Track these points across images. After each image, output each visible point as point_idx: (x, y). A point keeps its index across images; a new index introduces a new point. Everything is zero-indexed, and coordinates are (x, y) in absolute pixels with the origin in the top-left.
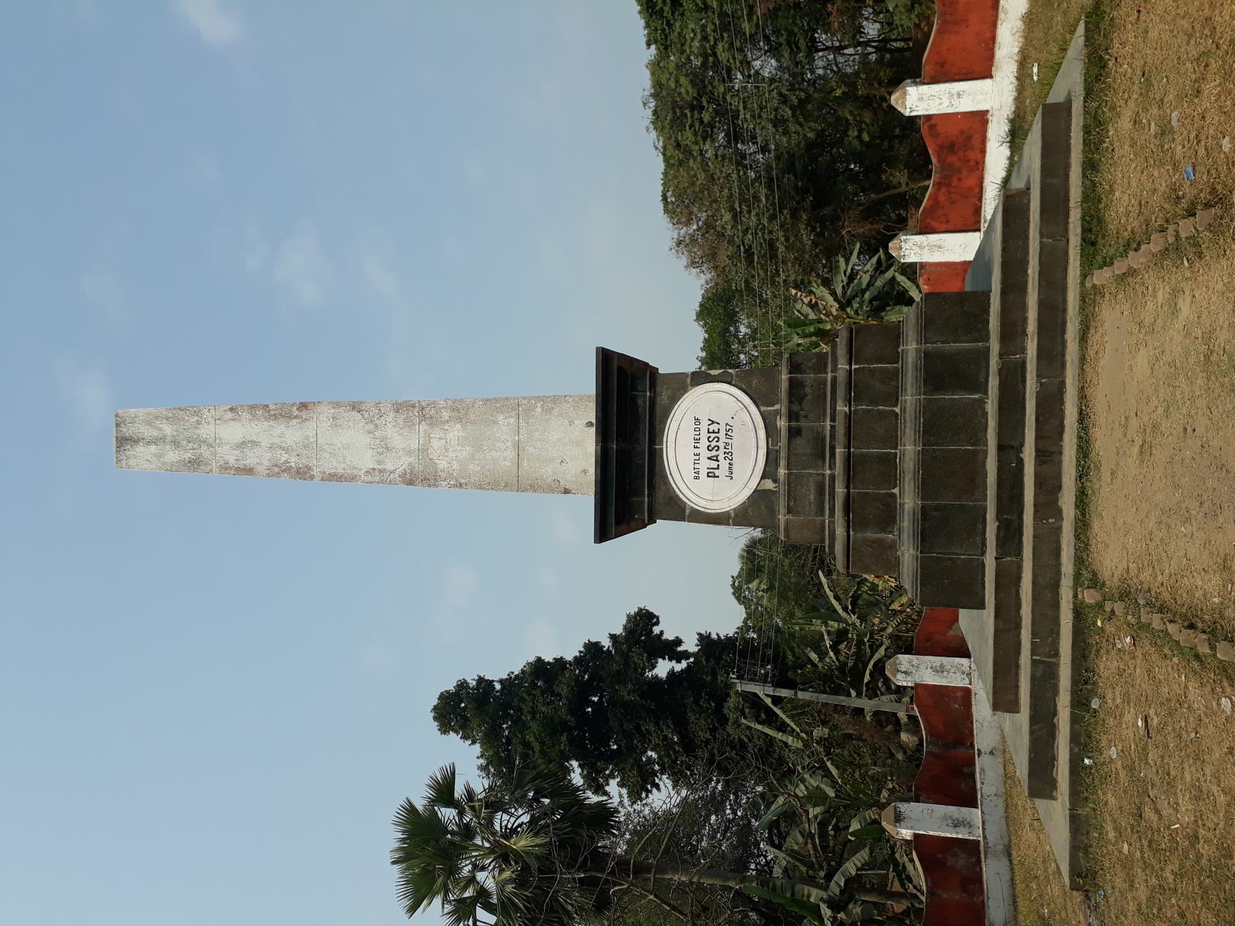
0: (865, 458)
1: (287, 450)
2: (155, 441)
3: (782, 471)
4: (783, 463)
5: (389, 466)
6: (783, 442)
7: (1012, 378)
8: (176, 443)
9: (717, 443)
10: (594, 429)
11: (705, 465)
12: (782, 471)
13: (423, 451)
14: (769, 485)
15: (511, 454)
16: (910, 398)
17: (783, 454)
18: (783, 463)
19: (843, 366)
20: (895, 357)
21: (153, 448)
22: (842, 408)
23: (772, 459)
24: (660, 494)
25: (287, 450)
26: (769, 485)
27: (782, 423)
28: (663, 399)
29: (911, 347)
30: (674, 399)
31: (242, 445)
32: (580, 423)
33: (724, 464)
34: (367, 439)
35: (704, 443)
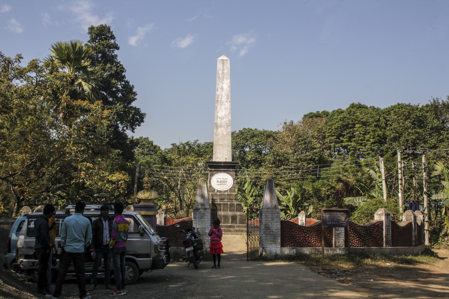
0: (221, 207)
1: (221, 98)
2: (223, 69)
3: (218, 193)
4: (220, 193)
5: (218, 119)
6: (223, 193)
7: (233, 227)
8: (223, 73)
9: (223, 182)
10: (224, 160)
11: (219, 180)
12: (218, 193)
13: (221, 126)
14: (216, 191)
15: (221, 143)
16: (230, 213)
17: (221, 193)
18: (220, 193)
19: (236, 203)
20: (236, 211)
21: (222, 68)
22: (229, 203)
23: (220, 192)
24: (214, 172)
25: (221, 98)
26: (216, 191)
27: (226, 193)
28: (231, 173)
29: (238, 213)
30: (230, 175)
31: (222, 88)
32: (227, 157)
33: (219, 183)
34: (223, 115)
35: (223, 180)
